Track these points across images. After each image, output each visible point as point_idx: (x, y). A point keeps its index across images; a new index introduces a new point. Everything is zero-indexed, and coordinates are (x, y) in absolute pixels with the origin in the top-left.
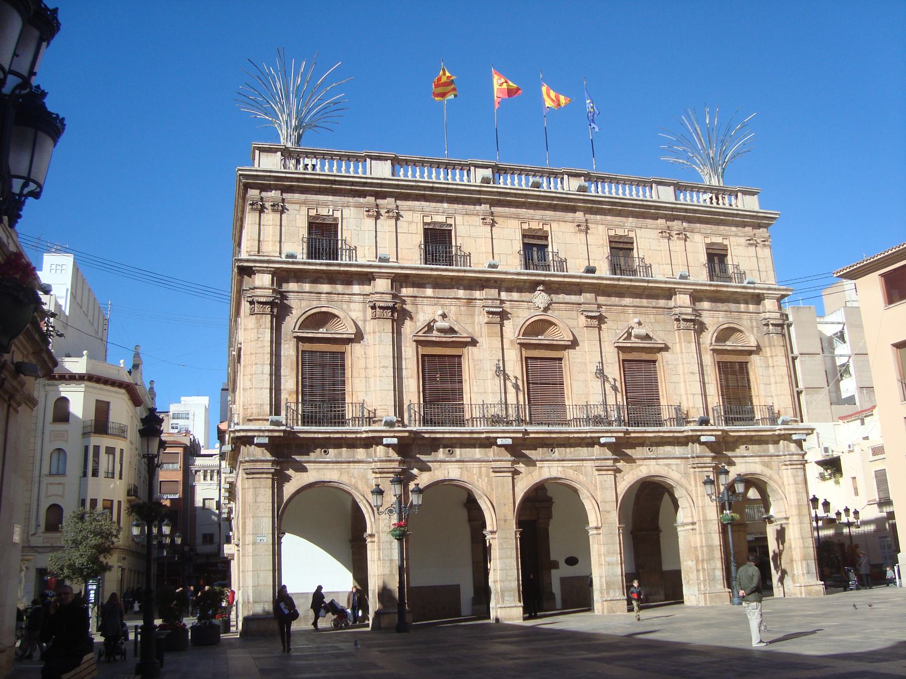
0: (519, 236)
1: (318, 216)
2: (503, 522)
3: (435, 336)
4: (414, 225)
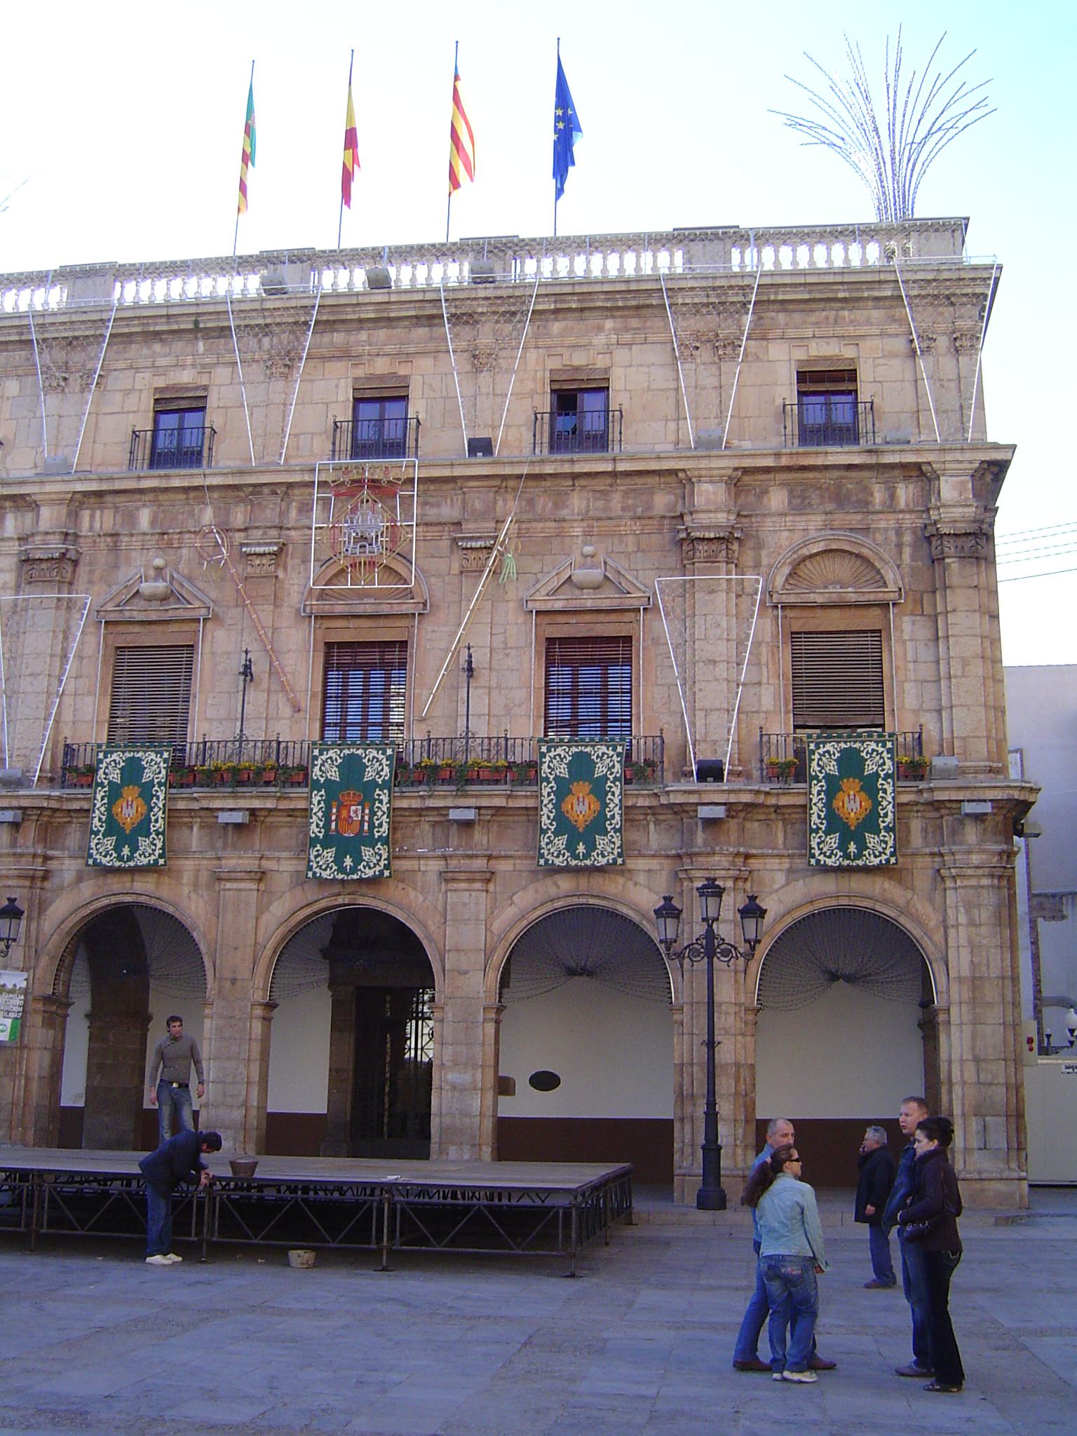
2: (228, 984)
3: (136, 612)
4: (133, 398)
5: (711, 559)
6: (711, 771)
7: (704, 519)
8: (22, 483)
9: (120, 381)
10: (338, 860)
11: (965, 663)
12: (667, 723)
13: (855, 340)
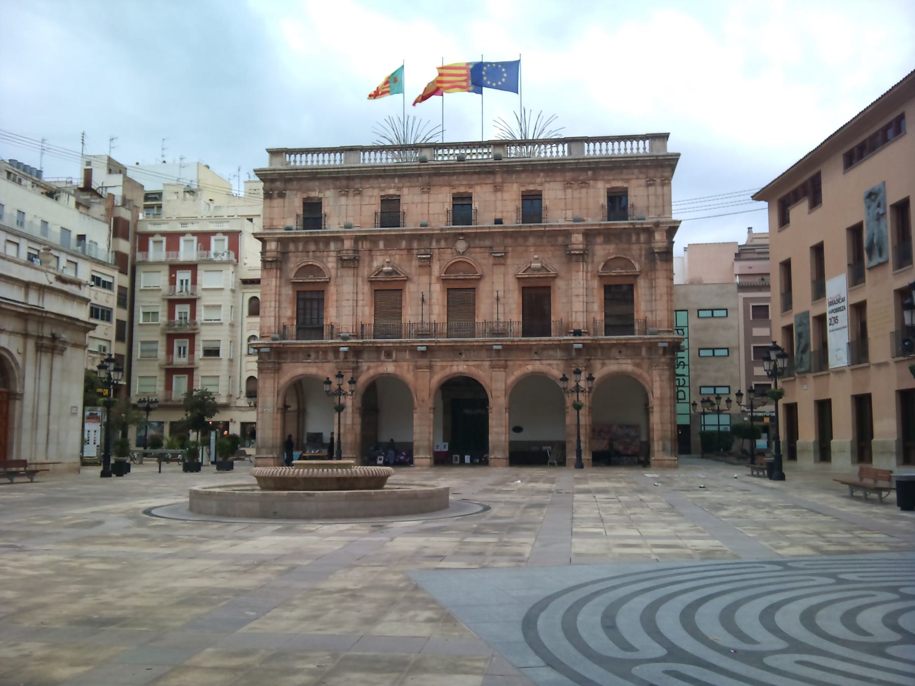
0: (449, 199)
1: (308, 198)
3: (381, 277)
5: (578, 261)
6: (578, 333)
7: (575, 247)
8: (338, 232)
9: (368, 192)
11: (661, 296)
12: (563, 316)
13: (627, 180)
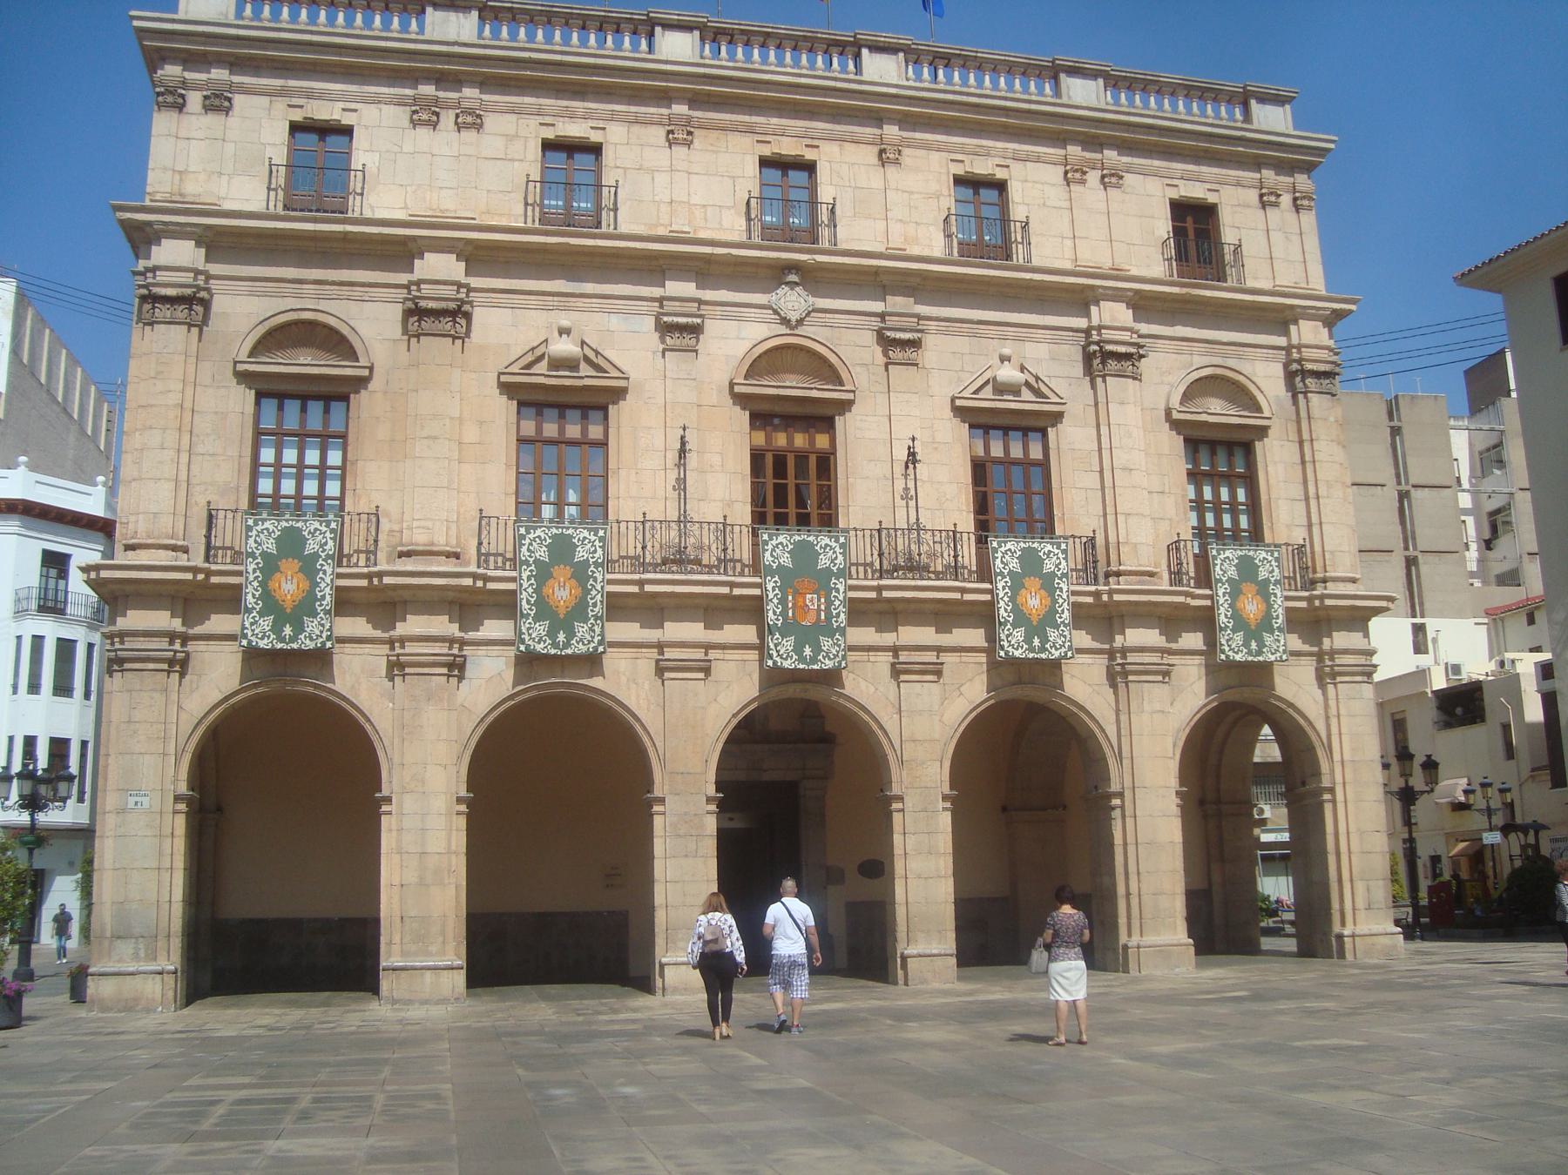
0: (752, 167)
3: (542, 375)
10: (798, 649)
